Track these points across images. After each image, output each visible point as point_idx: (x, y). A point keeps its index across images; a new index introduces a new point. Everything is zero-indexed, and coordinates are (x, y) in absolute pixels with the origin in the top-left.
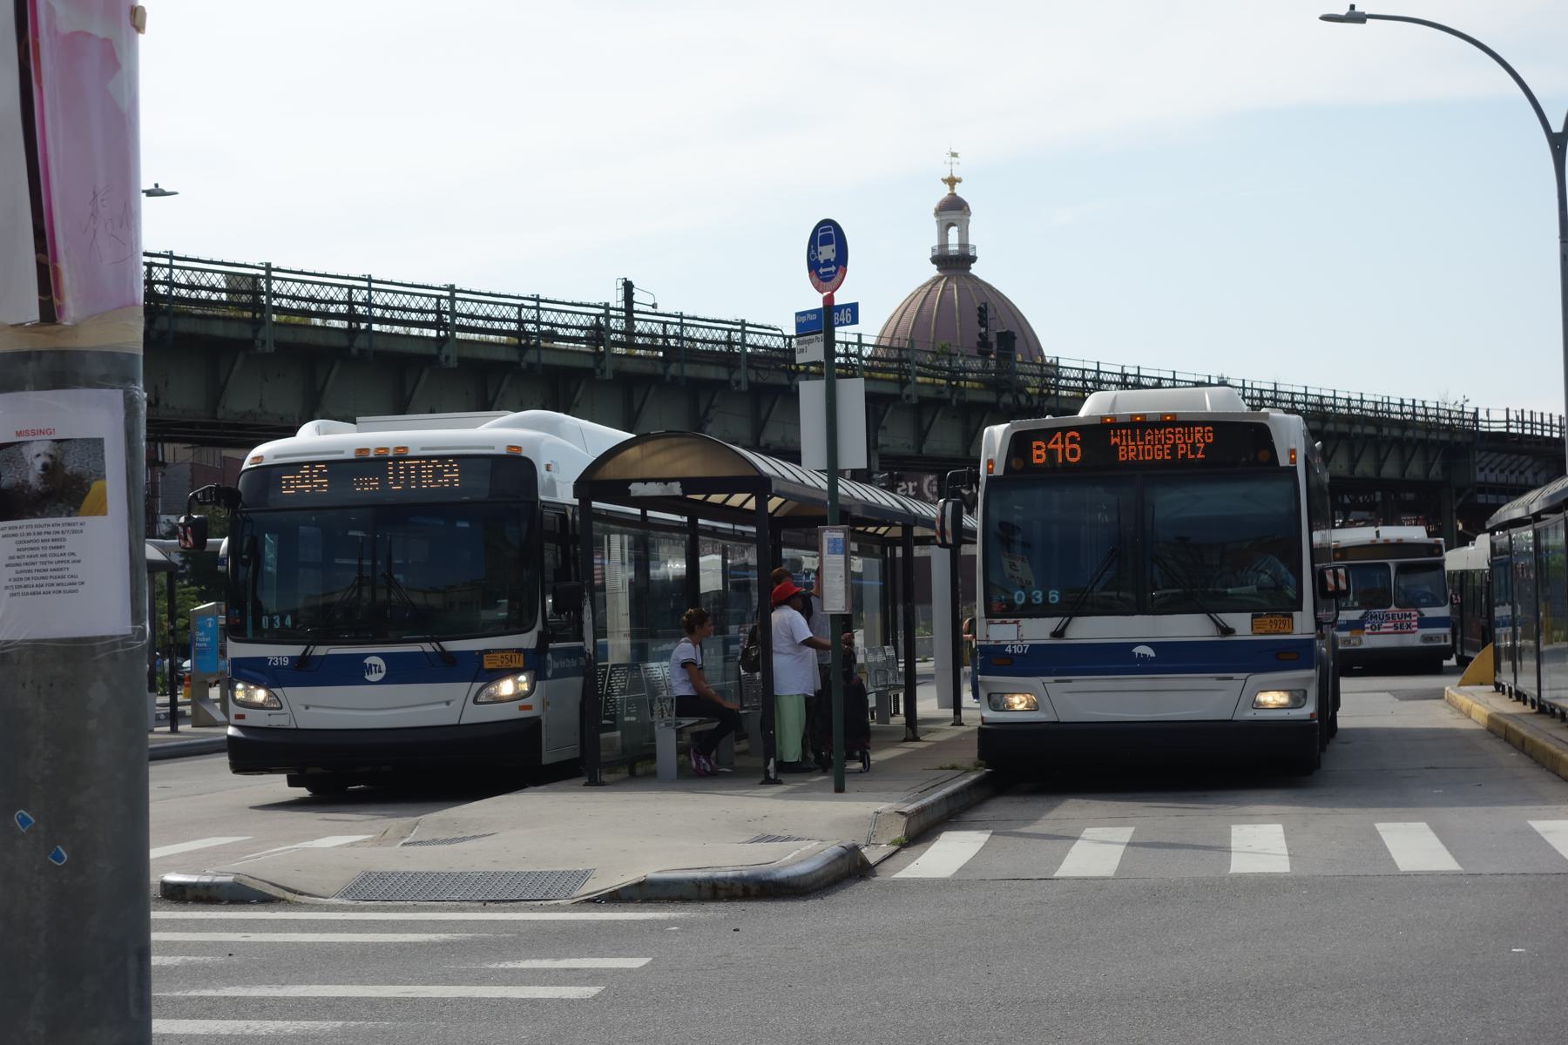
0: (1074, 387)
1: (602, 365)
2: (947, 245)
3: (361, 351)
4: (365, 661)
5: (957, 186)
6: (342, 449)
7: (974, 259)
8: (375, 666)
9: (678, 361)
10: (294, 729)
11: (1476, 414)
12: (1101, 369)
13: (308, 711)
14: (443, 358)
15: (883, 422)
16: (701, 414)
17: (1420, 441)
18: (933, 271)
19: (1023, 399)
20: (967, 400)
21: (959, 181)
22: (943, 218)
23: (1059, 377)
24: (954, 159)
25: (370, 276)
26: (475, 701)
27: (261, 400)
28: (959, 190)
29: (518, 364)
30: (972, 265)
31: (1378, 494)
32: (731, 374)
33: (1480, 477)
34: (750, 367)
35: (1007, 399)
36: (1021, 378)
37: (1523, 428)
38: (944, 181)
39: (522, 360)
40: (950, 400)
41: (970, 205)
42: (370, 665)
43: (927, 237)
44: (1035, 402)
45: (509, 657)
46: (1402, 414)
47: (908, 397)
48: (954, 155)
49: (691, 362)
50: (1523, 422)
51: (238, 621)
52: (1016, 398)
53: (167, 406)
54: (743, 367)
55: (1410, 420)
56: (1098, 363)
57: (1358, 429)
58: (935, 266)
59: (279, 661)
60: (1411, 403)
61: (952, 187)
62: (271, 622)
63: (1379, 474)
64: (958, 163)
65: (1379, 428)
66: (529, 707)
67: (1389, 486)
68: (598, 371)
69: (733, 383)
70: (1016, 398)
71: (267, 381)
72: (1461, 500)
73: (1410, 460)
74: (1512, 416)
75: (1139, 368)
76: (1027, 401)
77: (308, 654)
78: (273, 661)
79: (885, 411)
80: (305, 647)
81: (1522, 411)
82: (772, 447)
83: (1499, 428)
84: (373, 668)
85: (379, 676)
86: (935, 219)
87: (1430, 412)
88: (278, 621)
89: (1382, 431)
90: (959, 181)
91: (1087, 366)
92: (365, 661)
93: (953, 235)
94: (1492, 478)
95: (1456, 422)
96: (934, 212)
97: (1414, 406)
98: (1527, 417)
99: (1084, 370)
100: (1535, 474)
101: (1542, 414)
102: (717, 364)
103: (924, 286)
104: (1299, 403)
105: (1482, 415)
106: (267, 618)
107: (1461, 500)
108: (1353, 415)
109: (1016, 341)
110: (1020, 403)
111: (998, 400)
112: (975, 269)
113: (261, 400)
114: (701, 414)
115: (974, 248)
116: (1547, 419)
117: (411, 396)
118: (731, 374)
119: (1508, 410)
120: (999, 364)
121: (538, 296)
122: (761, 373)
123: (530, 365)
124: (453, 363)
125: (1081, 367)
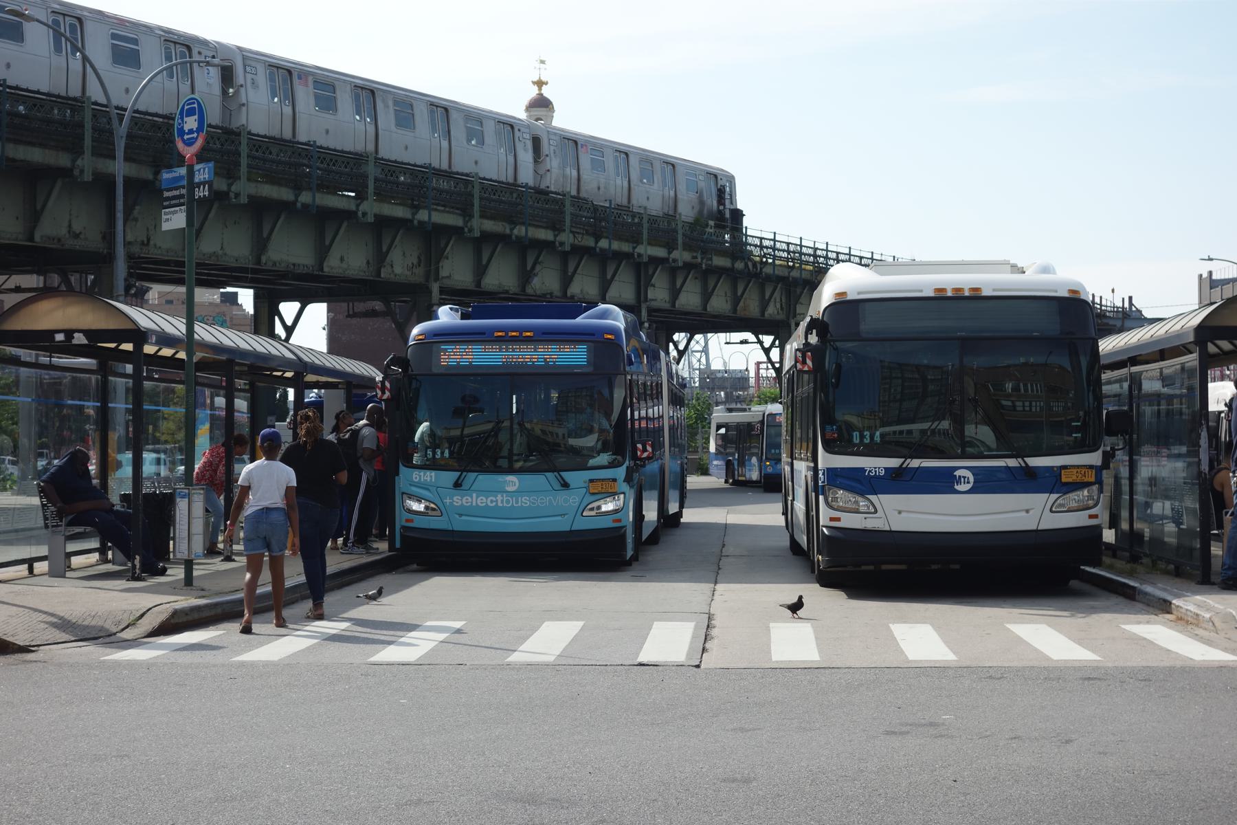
0: (781, 257)
1: (469, 224)
3: (305, 206)
4: (955, 474)
5: (544, 87)
6: (920, 289)
8: (964, 477)
9: (523, 224)
10: (888, 531)
12: (803, 244)
13: (898, 515)
14: (360, 214)
15: (653, 280)
16: (529, 268)
19: (750, 264)
20: (713, 264)
21: (546, 83)
22: (532, 113)
23: (774, 249)
24: (542, 65)
25: (315, 142)
26: (1051, 511)
27: (222, 244)
28: (546, 92)
29: (411, 221)
32: (556, 236)
34: (572, 232)
35: (739, 265)
36: (748, 247)
38: (534, 83)
39: (413, 218)
40: (701, 264)
41: (554, 104)
42: (960, 477)
44: (759, 269)
45: (1083, 472)
47: (675, 261)
48: (543, 62)
49: (530, 225)
51: (836, 435)
52: (746, 265)
53: (155, 245)
54: (567, 230)
56: (801, 238)
59: (876, 471)
61: (540, 89)
62: (862, 437)
64: (545, 69)
66: (1096, 516)
68: (466, 230)
69: (557, 244)
70: (746, 265)
71: (227, 227)
75: (827, 244)
76: (753, 268)
77: (904, 466)
78: (870, 471)
79: (654, 273)
80: (903, 459)
82: (576, 298)
84: (962, 479)
85: (968, 487)
88: (868, 437)
90: (546, 83)
91: (791, 240)
92: (955, 474)
96: (525, 108)
99: (788, 244)
102: (546, 228)
106: (858, 433)
109: (745, 218)
110: (749, 269)
111: (733, 265)
113: (222, 244)
114: (529, 268)
117: (331, 245)
118: (556, 236)
120: (733, 237)
121: (430, 164)
122: (577, 235)
123: (420, 222)
124: (371, 219)
125: (787, 241)
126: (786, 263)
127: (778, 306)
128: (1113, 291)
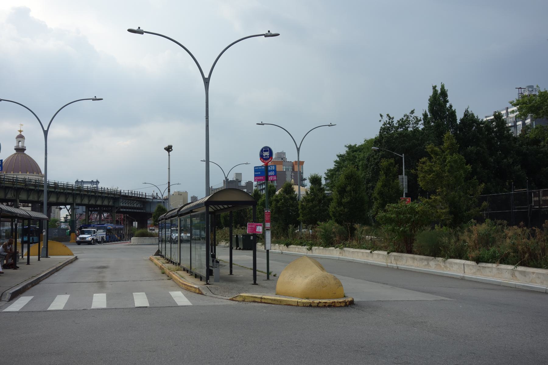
2: (19, 146)
5: (22, 132)
7: (25, 150)
11: (121, 191)
17: (106, 197)
18: (15, 152)
21: (22, 131)
24: (21, 126)
28: (22, 133)
30: (25, 151)
31: (99, 208)
33: (121, 205)
37: (132, 195)
43: (14, 144)
46: (102, 190)
50: (132, 193)
55: (103, 192)
57: (89, 193)
58: (15, 151)
60: (104, 188)
63: (96, 203)
65: (95, 193)
67: (100, 206)
72: (117, 210)
73: (104, 200)
74: (130, 192)
81: (132, 191)
83: (127, 194)
86: (16, 140)
87: (109, 190)
89: (96, 194)
90: (22, 131)
93: (20, 144)
94: (124, 205)
95: (115, 193)
97: (104, 189)
98: (133, 192)
99: (13, 177)
100: (137, 205)
101: (137, 192)
103: (12, 155)
104: (74, 187)
105: (122, 191)
107: (117, 210)
108: (81, 189)
112: (25, 152)
115: (25, 147)
116: (138, 193)
119: (128, 191)
126: (12, 183)
127: (13, 195)
128: (154, 191)
